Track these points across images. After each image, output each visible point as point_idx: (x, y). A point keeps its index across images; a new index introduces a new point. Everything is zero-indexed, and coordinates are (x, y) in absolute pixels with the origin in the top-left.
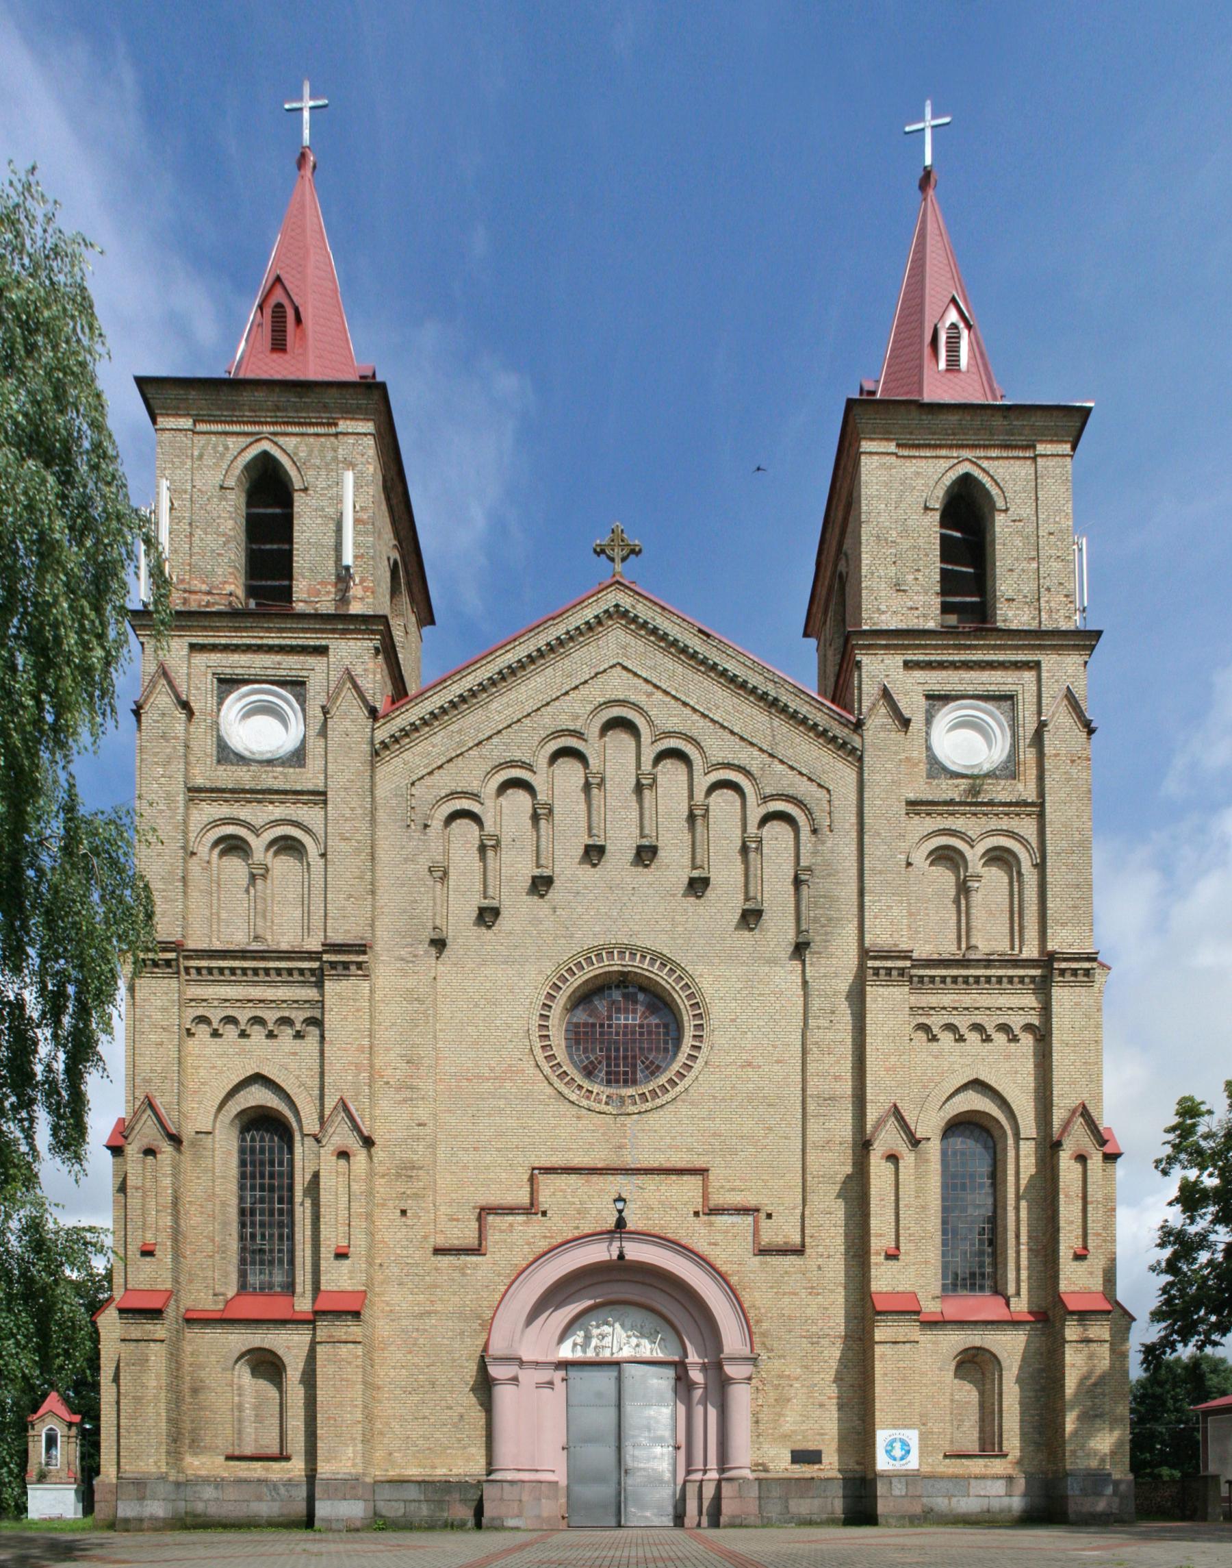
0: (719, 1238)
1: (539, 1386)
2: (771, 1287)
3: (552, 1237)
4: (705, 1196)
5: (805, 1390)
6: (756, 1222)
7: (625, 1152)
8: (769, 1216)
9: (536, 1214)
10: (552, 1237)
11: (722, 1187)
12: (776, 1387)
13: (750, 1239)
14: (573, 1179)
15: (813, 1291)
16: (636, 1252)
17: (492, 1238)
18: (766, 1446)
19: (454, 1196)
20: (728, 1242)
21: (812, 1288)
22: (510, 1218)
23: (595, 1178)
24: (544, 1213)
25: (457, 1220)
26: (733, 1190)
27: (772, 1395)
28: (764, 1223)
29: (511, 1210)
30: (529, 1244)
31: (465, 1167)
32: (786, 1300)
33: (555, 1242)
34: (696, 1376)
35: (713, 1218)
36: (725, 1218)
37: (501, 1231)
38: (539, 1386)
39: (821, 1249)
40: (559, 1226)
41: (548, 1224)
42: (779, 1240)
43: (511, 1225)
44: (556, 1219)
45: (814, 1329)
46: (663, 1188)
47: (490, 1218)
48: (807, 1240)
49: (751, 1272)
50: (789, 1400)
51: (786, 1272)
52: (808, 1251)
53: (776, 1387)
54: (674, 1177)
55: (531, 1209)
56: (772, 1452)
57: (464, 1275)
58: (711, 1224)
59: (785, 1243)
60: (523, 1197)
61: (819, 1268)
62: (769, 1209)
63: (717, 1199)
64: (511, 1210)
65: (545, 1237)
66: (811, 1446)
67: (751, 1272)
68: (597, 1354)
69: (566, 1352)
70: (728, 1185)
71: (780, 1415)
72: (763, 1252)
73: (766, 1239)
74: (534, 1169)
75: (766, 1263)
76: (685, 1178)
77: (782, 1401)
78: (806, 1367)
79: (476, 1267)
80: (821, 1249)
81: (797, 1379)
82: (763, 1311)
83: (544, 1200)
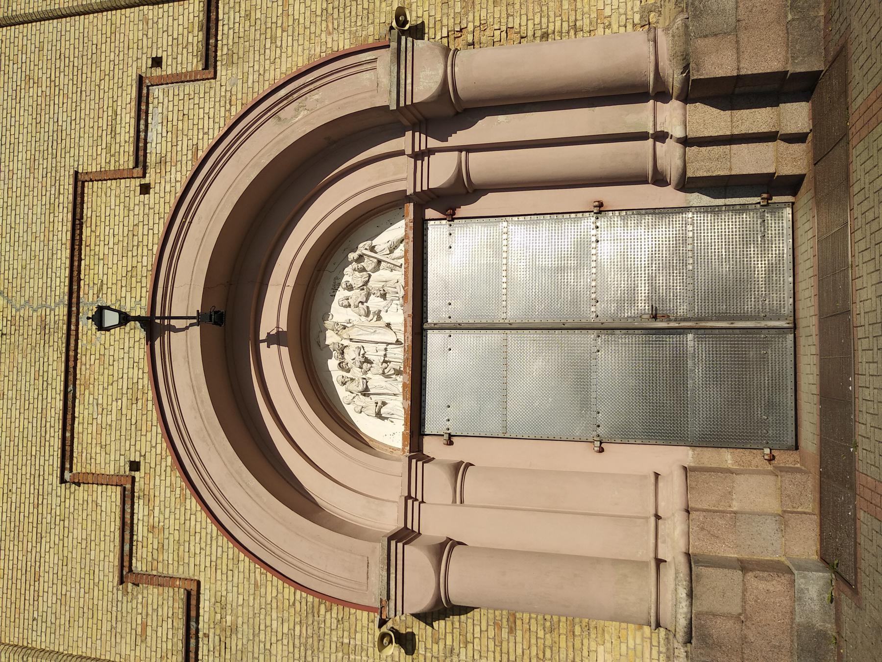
1: (459, 498)
2: (273, 40)
4: (117, 176)
7: (51, 319)
8: (157, 62)
9: (133, 478)
11: (108, 148)
13: (189, 88)
16: (187, 296)
19: (106, 626)
20: (187, 121)
22: (140, 530)
24: (135, 466)
25: (144, 626)
29: (127, 526)
31: (62, 600)
34: (440, 171)
35: (151, 159)
36: (152, 136)
37: (161, 548)
38: (459, 498)
41: (151, 458)
44: (143, 445)
46: (102, 250)
47: (138, 566)
51: (248, 16)
54: (86, 232)
57: (234, 629)
58: (162, 161)
60: (110, 499)
62: (145, 63)
63: (126, 160)
64: (127, 526)
68: (398, 372)
69: (391, 433)
70: (106, 139)
72: (209, 60)
73: (192, 63)
74: (63, 481)
75: (231, 54)
79: (221, 604)
83: (112, 463)
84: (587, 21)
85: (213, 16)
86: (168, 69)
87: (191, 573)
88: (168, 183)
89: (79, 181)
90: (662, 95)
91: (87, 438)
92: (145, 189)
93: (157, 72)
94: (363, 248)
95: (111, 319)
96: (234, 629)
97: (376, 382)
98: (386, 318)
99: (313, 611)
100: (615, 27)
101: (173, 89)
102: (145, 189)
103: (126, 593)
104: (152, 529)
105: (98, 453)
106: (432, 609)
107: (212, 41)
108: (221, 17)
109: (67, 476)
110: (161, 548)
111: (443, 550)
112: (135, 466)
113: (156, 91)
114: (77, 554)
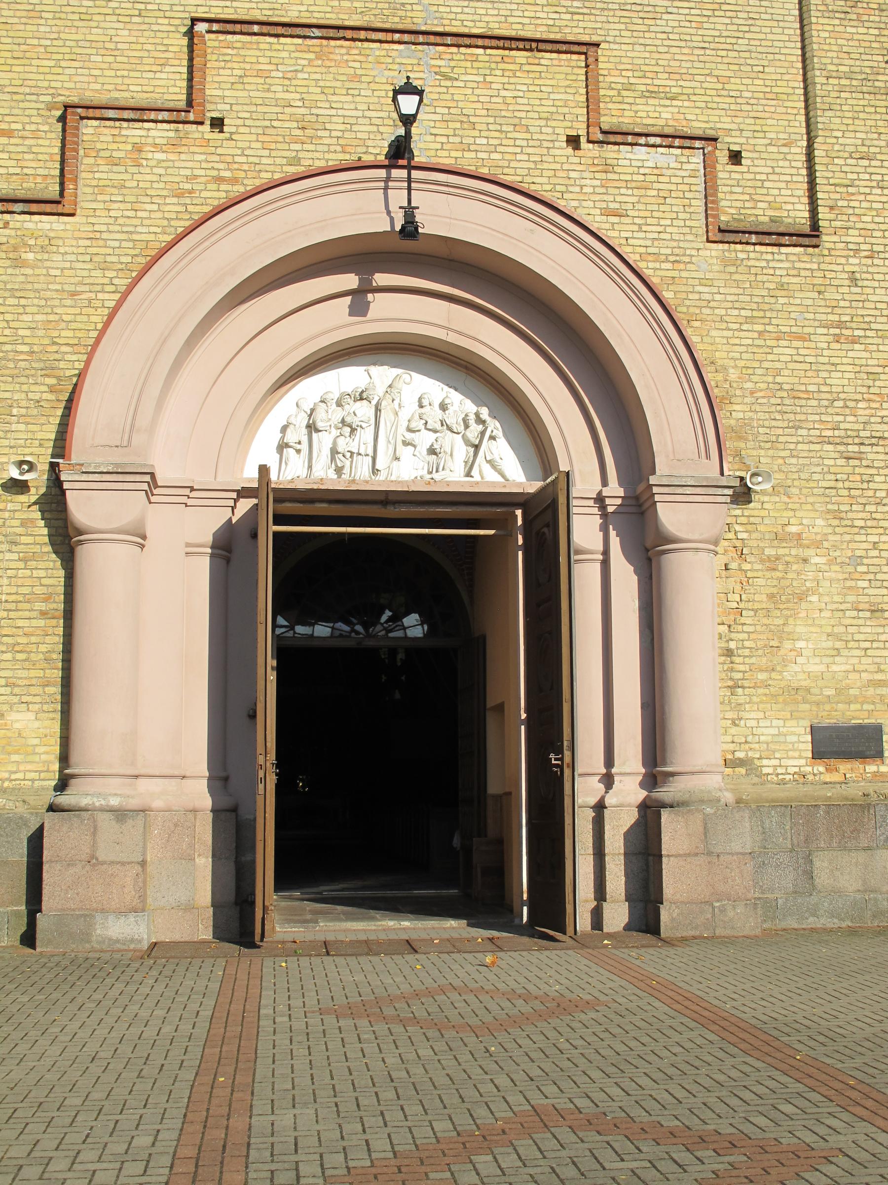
0: (628, 197)
2: (749, 320)
3: (234, 181)
4: (591, 103)
5: (835, 572)
6: (709, 165)
8: (735, 157)
9: (202, 123)
10: (234, 181)
11: (629, 87)
12: (772, 564)
13: (699, 204)
14: (286, 47)
15: (842, 333)
17: (90, 174)
18: (751, 715)
21: (840, 325)
22: (134, 132)
23: (339, 49)
24: (218, 124)
26: (653, 94)
27: (763, 583)
28: (725, 171)
29: (139, 113)
30: (179, 194)
32: (784, 351)
33: (239, 189)
35: (610, 151)
36: (641, 152)
37: (114, 162)
39: (853, 237)
40: (249, 153)
42: (762, 215)
43: (138, 149)
45: (850, 423)
46: (497, 80)
47: (89, 129)
48: (823, 213)
49: (702, 282)
50: (802, 597)
51: (781, 286)
52: (827, 239)
53: (772, 564)
55: (189, 110)
56: (767, 731)
57: (19, 263)
58: (608, 167)
59: (773, 220)
61: (853, 280)
64: (139, 113)
65: (219, 180)
66: (856, 714)
67: (702, 282)
71: (781, 634)
72: (728, 234)
73: (730, 209)
74: (194, 21)
75: (736, 263)
76: (547, 58)
77: (787, 599)
78: (837, 515)
80: (853, 237)
81: (818, 545)
82: (733, 374)
83: (218, 94)
84: (742, 700)
85: (786, 240)
86: (725, 171)
87: (85, 204)
88: (577, 182)
89: (587, 48)
90: (653, 778)
91: (251, 54)
92: (573, 141)
93: (722, 157)
94: (494, 426)
95: (408, 104)
96: (19, 263)
97: (324, 441)
98: (405, 453)
99: (49, 370)
100: (734, 730)
101: (699, 183)
102: (573, 141)
103: (50, 107)
104: (138, 149)
105: (231, 68)
106: (72, 524)
107: (754, 239)
108: (784, 250)
109: (201, 27)
110: (114, 162)
111: (139, 535)
112: (218, 124)
113: (697, 159)
114: (96, 34)
